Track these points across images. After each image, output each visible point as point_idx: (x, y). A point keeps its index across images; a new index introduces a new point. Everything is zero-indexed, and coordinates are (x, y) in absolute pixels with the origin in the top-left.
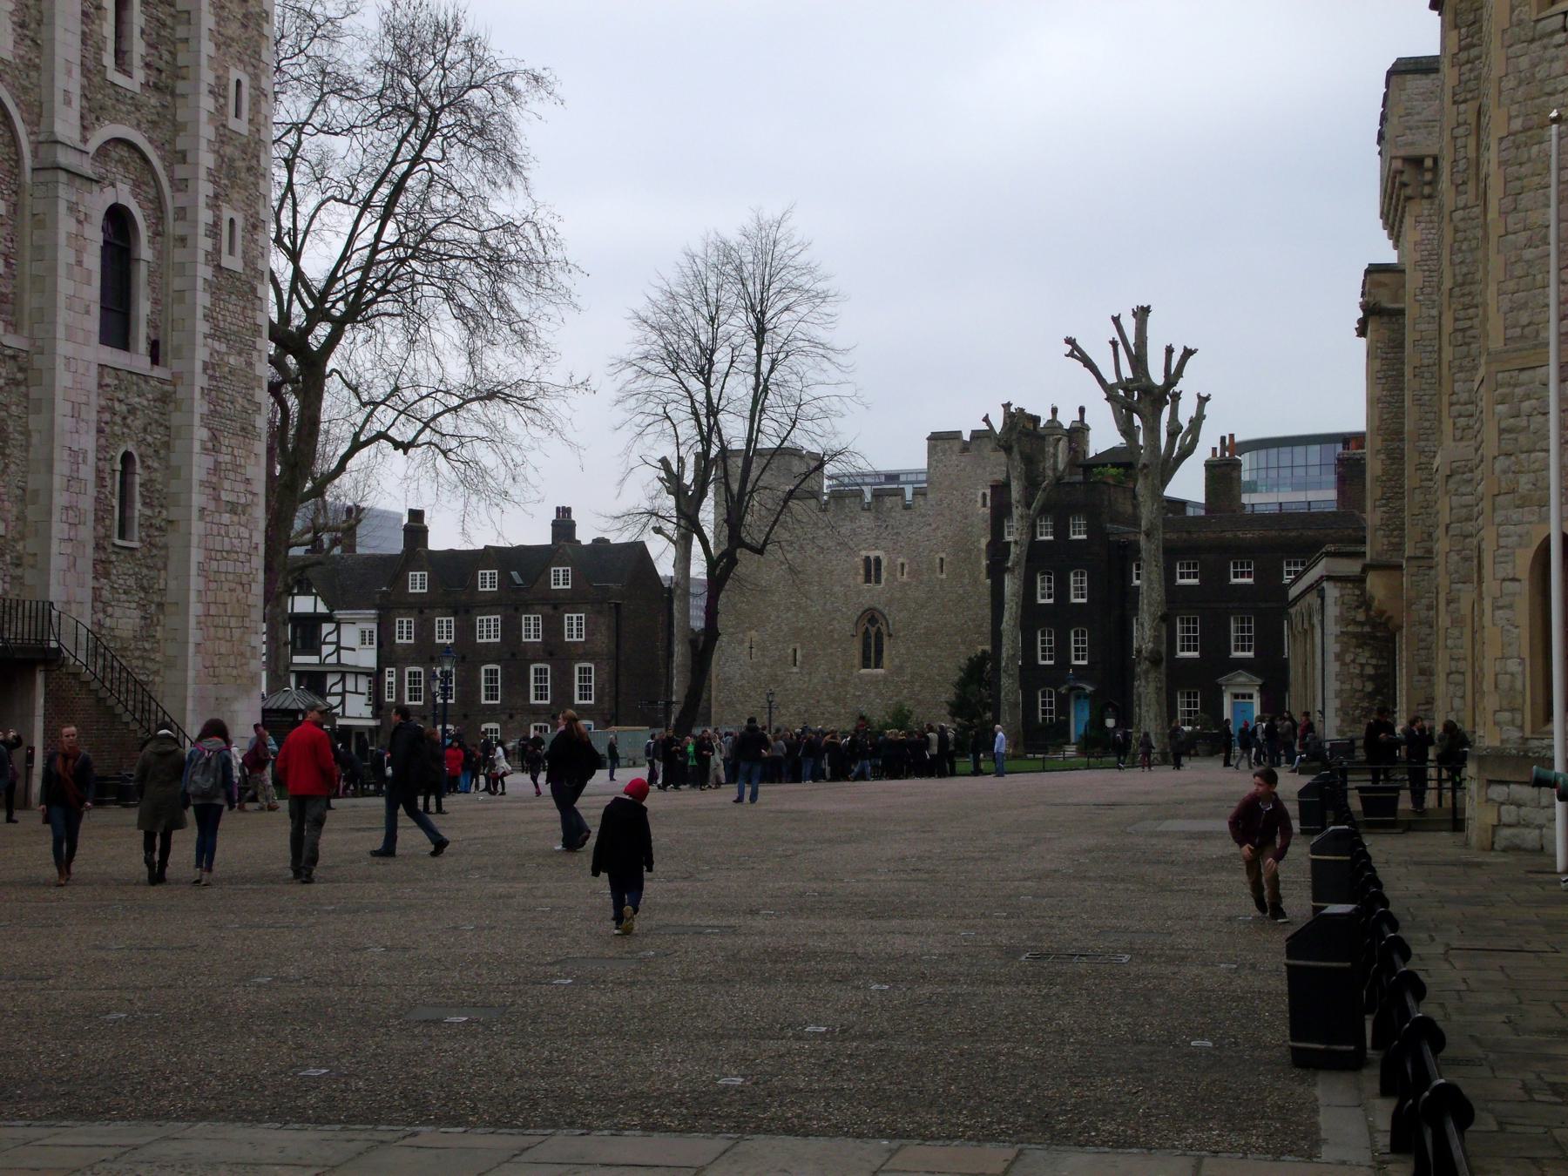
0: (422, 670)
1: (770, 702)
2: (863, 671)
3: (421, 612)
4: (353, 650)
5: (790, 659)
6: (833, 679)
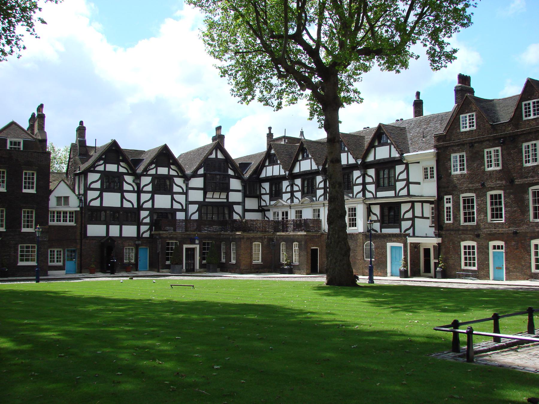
4: (419, 183)
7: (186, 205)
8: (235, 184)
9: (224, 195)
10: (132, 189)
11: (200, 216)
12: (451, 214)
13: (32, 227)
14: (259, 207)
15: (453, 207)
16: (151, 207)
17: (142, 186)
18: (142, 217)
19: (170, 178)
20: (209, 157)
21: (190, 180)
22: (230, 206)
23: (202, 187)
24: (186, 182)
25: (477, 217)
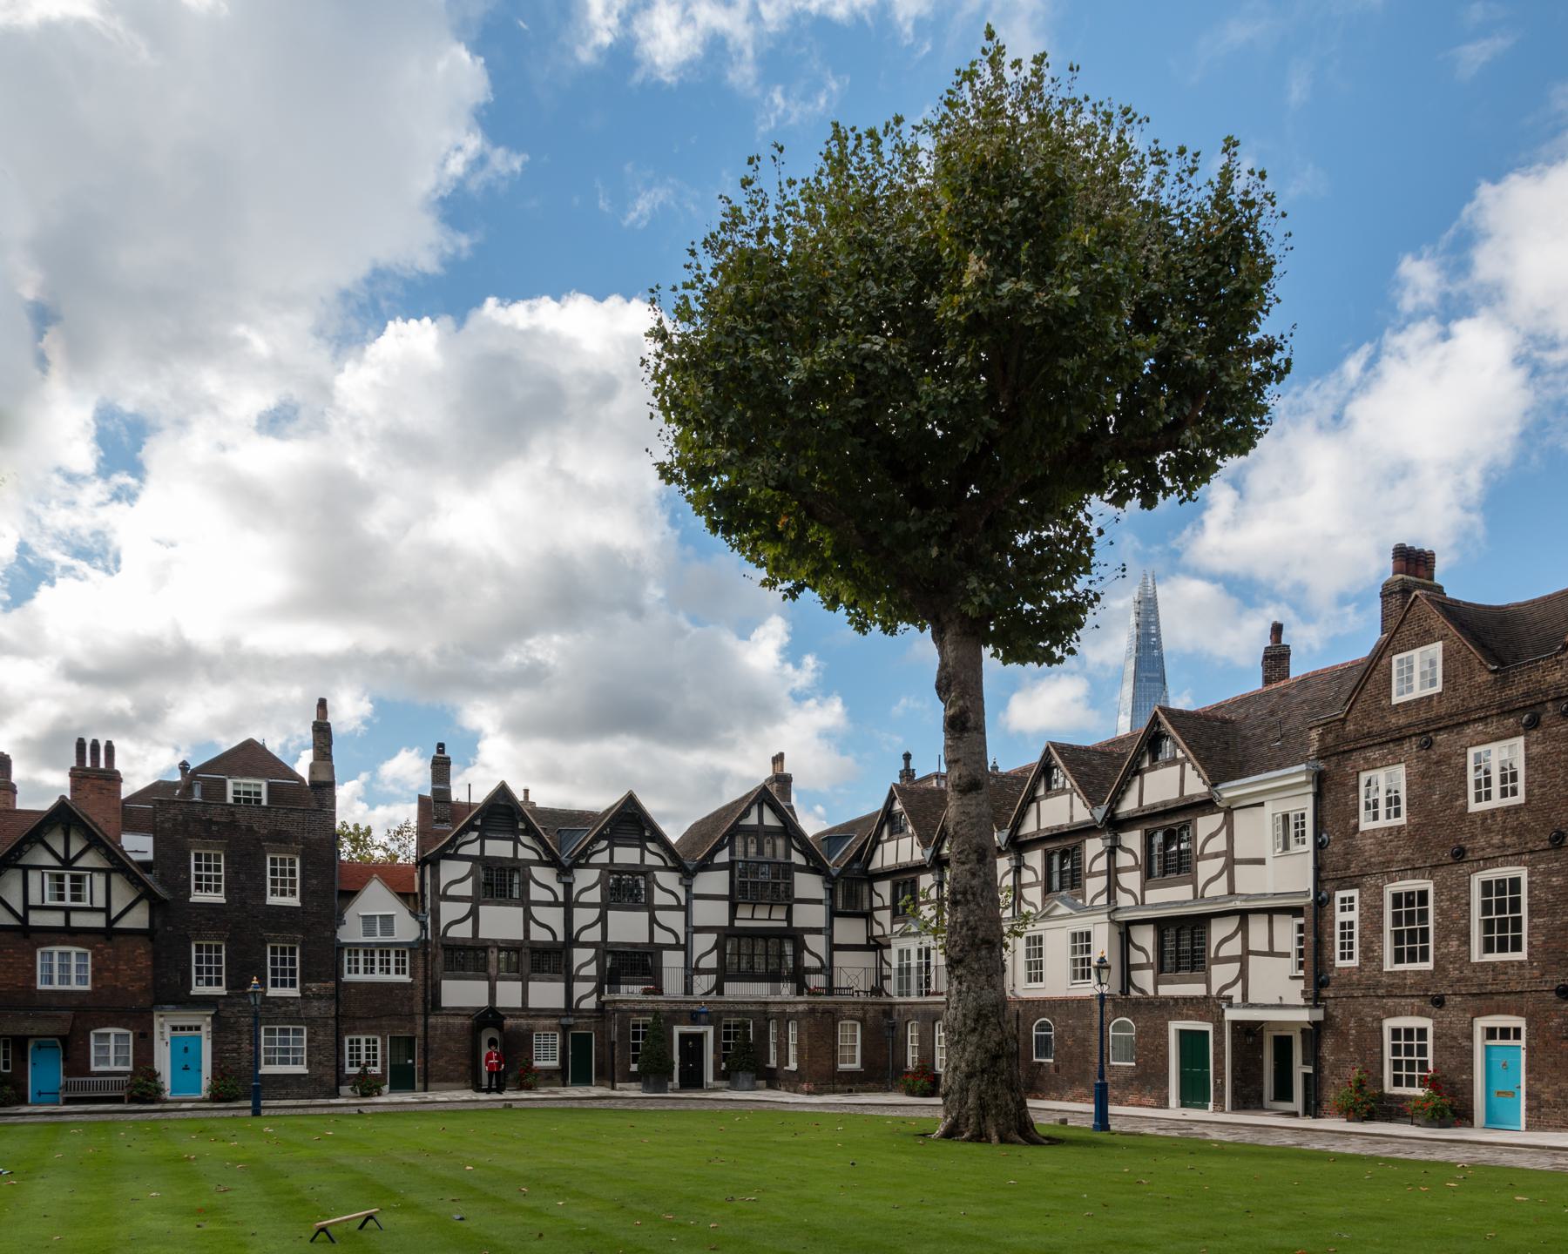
0: (1429, 885)
7: (686, 934)
8: (808, 885)
9: (779, 913)
10: (549, 897)
11: (721, 959)
12: (1356, 940)
13: (293, 984)
14: (868, 938)
15: (1361, 921)
16: (599, 939)
17: (575, 891)
18: (575, 966)
19: (647, 872)
20: (742, 823)
21: (693, 876)
22: (795, 936)
23: (727, 893)
24: (685, 882)
25: (1437, 948)
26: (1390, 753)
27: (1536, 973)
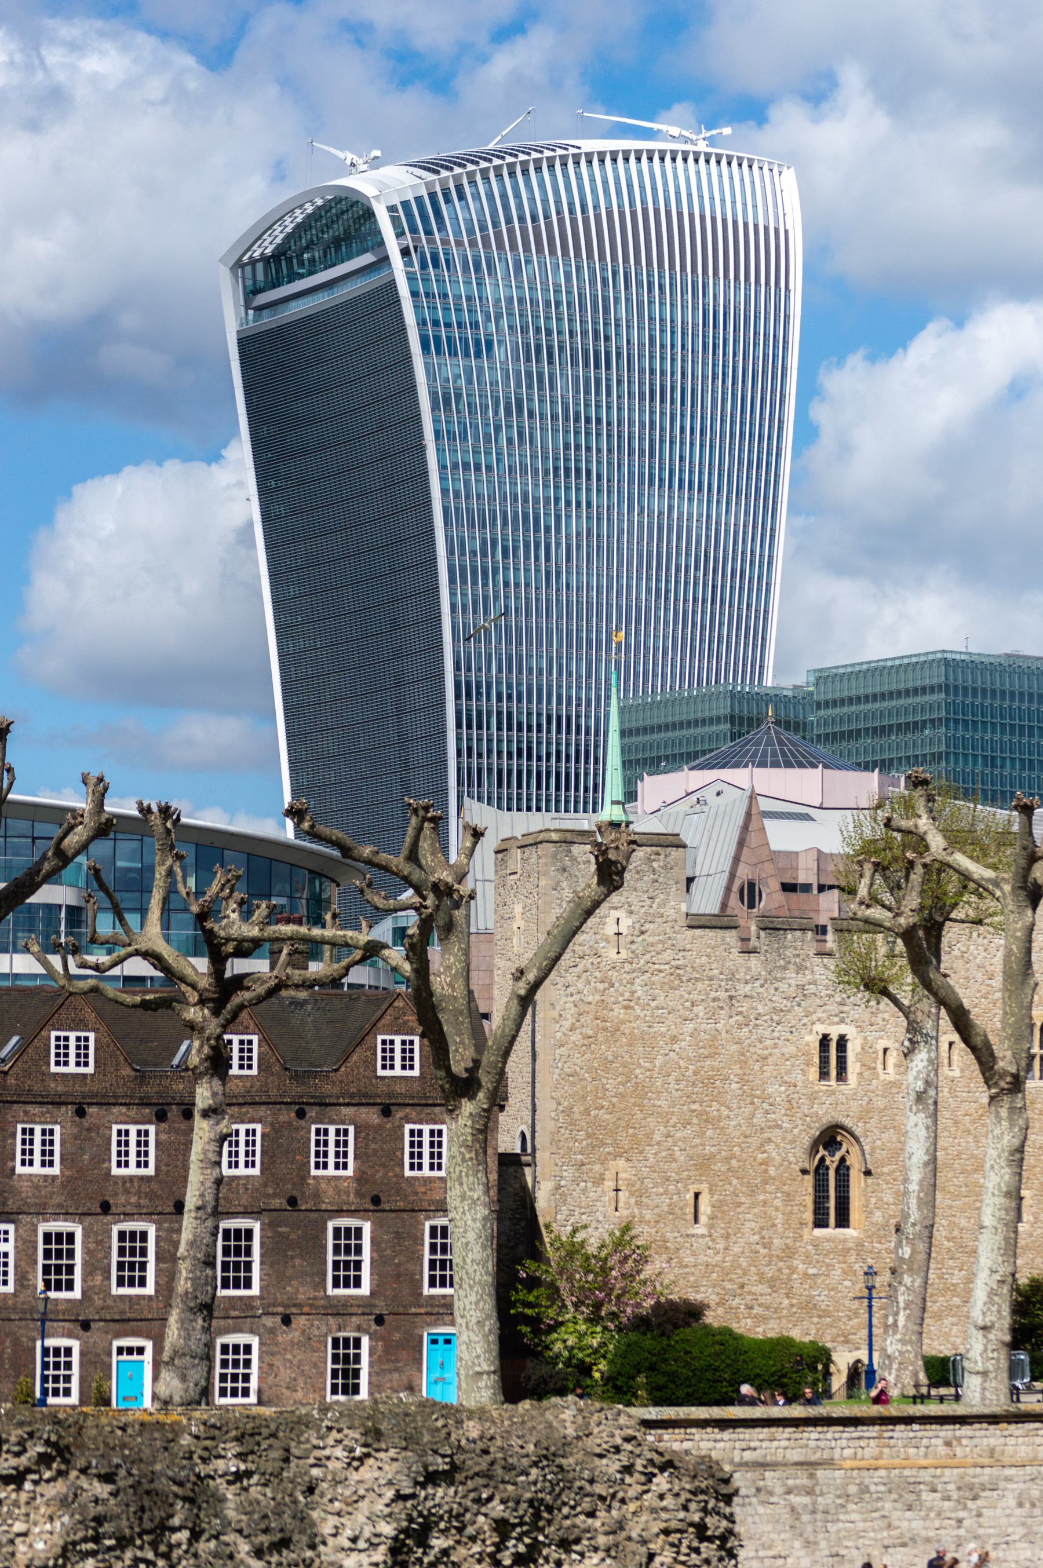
1: (870, 1289)
2: (819, 1232)
3: (81, 1113)
5: (690, 1210)
6: (767, 1246)
25: (84, 1280)
26: (48, 1112)
27: (161, 1305)
